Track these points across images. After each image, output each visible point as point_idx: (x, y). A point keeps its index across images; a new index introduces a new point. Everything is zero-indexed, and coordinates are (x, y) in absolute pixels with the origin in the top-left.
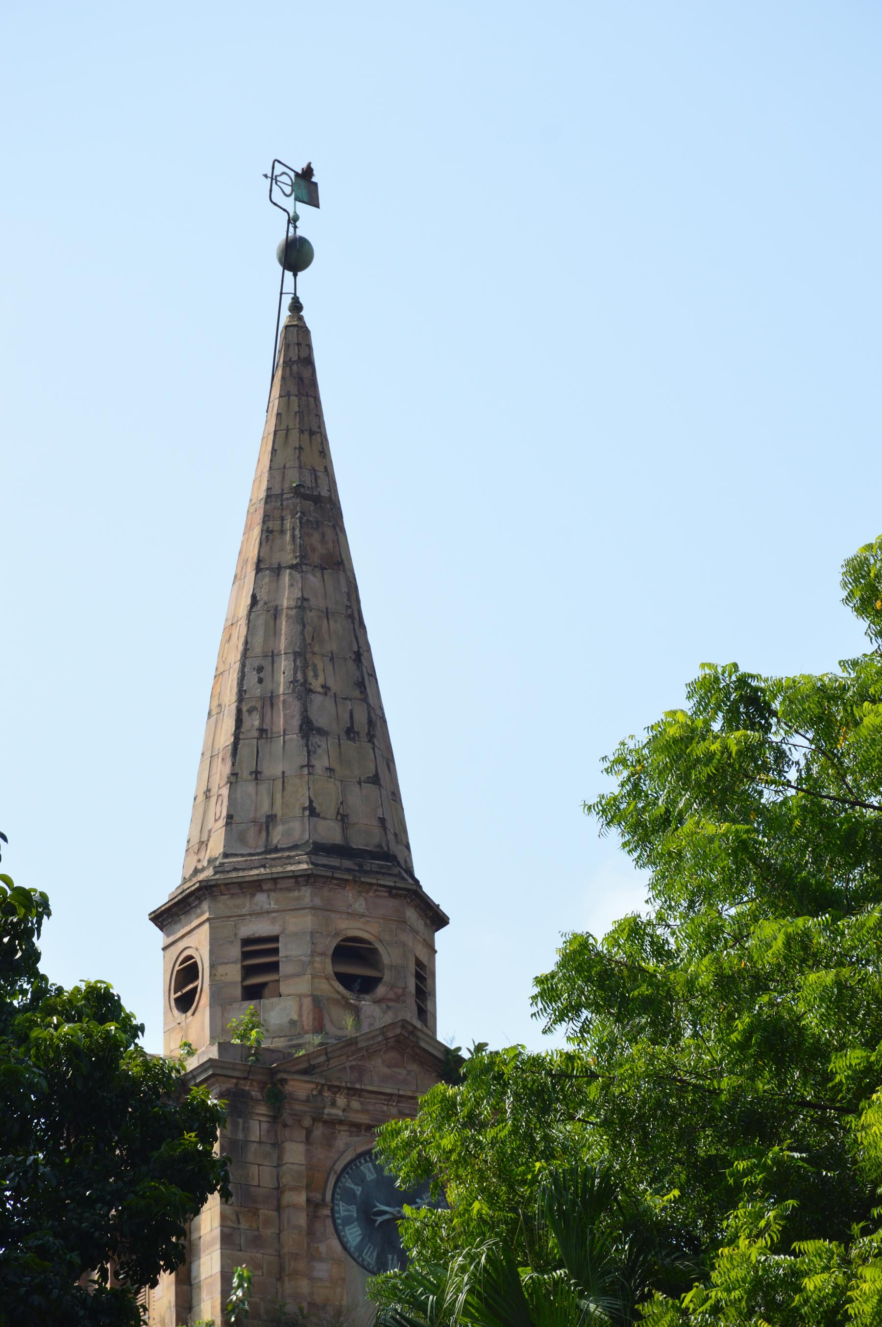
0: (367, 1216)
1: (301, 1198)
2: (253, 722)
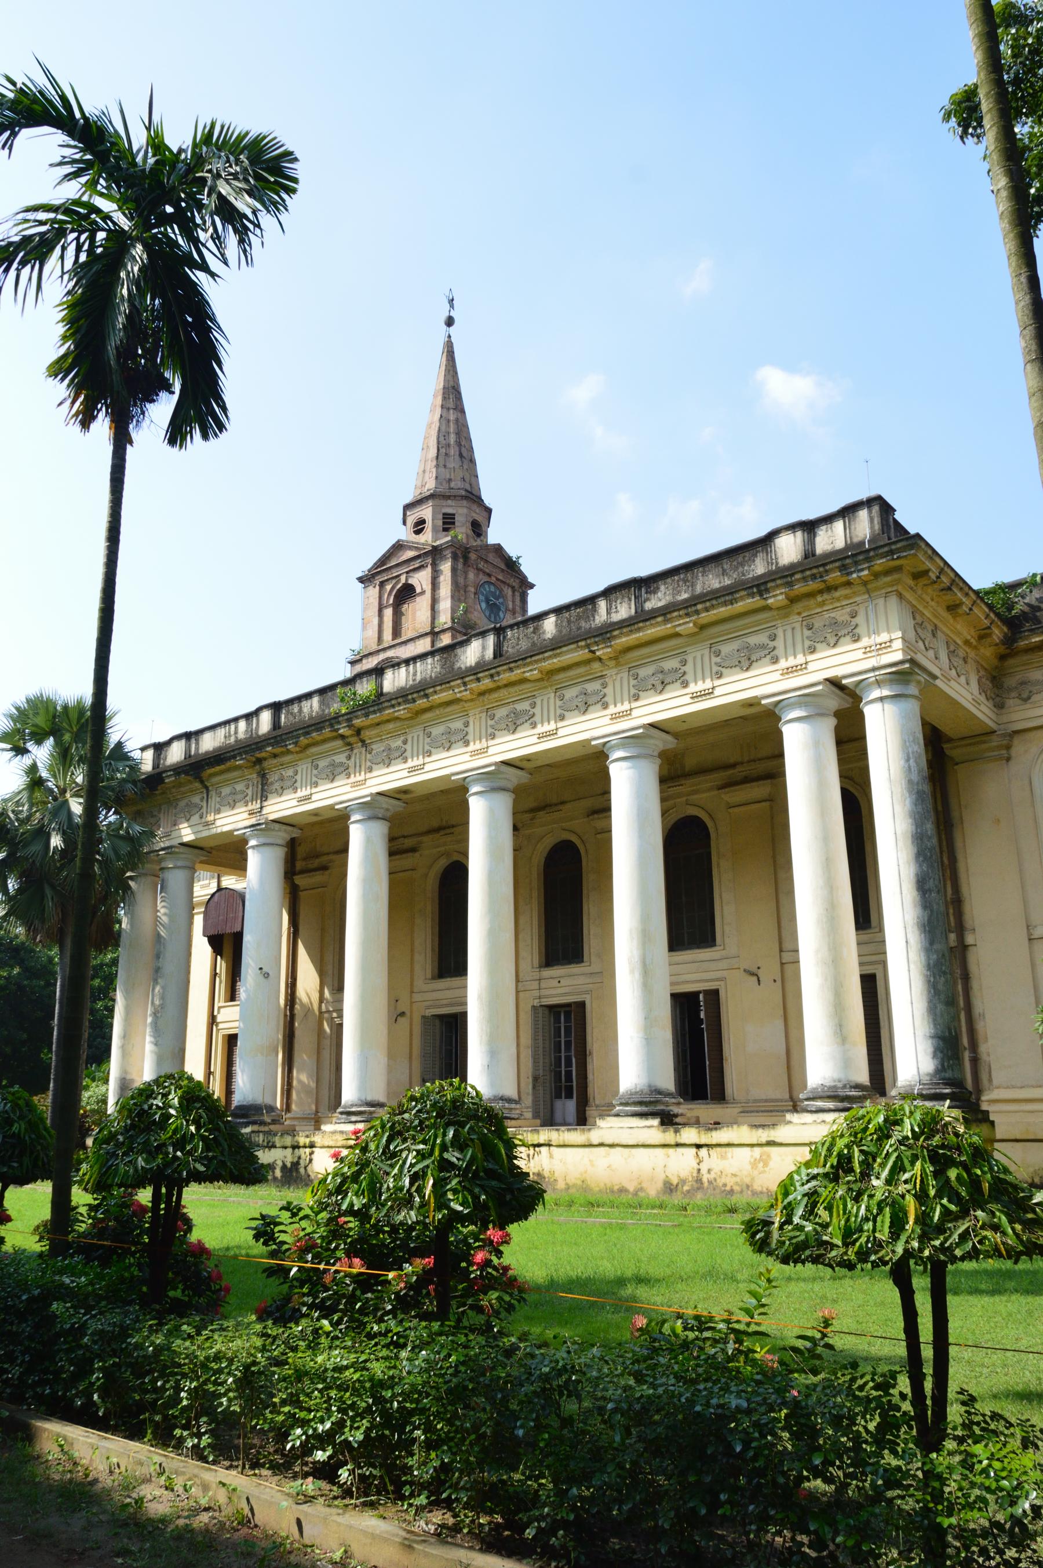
0: (487, 601)
1: (473, 590)
2: (443, 451)
